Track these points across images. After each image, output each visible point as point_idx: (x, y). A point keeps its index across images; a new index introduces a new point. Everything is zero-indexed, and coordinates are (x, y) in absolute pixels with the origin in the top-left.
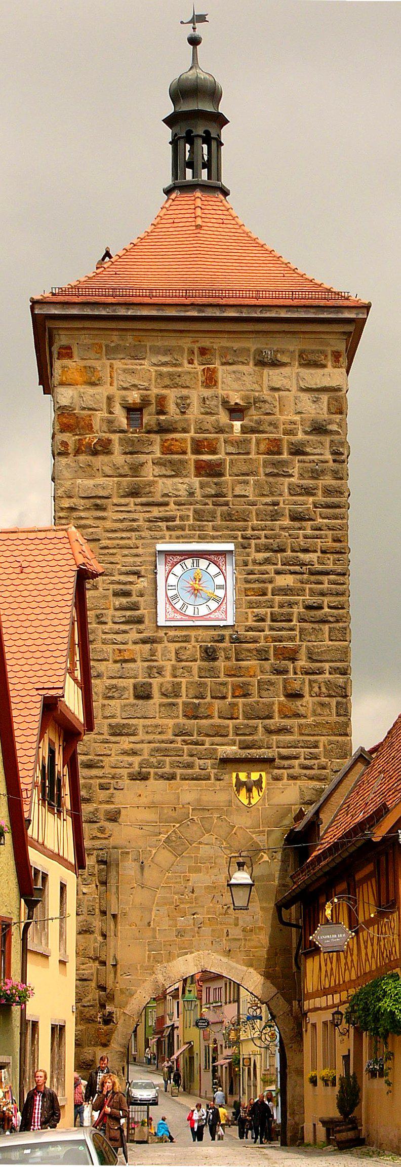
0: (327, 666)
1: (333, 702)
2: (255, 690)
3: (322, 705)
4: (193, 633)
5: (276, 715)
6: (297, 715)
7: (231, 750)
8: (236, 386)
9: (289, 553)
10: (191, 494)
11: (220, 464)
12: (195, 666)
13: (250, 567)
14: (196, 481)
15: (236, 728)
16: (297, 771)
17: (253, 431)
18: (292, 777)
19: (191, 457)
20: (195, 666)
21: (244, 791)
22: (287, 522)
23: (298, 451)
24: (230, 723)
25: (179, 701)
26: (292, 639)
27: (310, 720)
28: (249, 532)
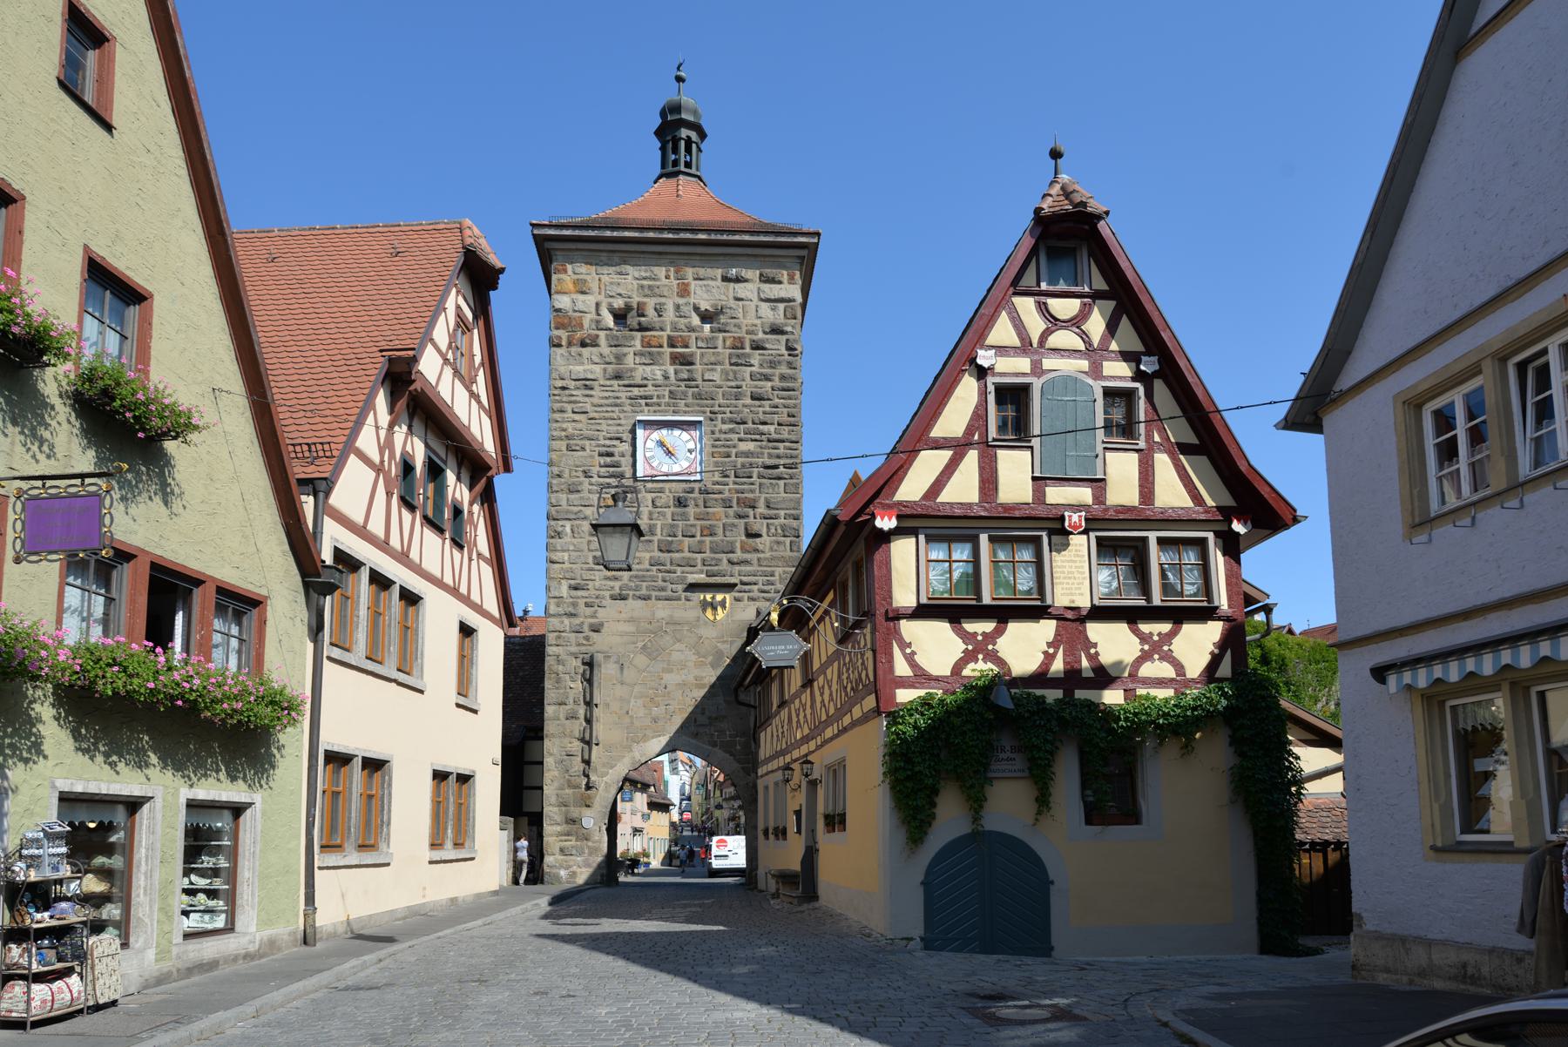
0: (782, 513)
1: (788, 540)
2: (720, 531)
3: (778, 543)
4: (667, 486)
5: (738, 550)
6: (757, 551)
7: (701, 578)
8: (705, 296)
9: (750, 425)
10: (666, 378)
11: (692, 355)
12: (668, 512)
13: (717, 435)
14: (671, 370)
15: (704, 560)
16: (756, 594)
17: (720, 331)
18: (751, 599)
19: (667, 350)
20: (668, 512)
21: (709, 610)
22: (748, 401)
23: (757, 346)
24: (699, 556)
25: (655, 539)
26: (752, 491)
27: (768, 555)
28: (716, 409)
